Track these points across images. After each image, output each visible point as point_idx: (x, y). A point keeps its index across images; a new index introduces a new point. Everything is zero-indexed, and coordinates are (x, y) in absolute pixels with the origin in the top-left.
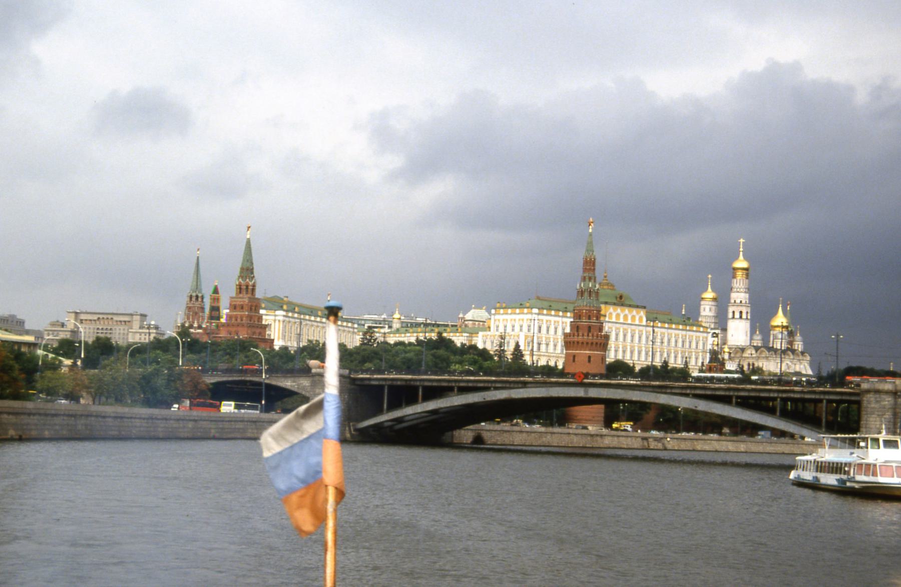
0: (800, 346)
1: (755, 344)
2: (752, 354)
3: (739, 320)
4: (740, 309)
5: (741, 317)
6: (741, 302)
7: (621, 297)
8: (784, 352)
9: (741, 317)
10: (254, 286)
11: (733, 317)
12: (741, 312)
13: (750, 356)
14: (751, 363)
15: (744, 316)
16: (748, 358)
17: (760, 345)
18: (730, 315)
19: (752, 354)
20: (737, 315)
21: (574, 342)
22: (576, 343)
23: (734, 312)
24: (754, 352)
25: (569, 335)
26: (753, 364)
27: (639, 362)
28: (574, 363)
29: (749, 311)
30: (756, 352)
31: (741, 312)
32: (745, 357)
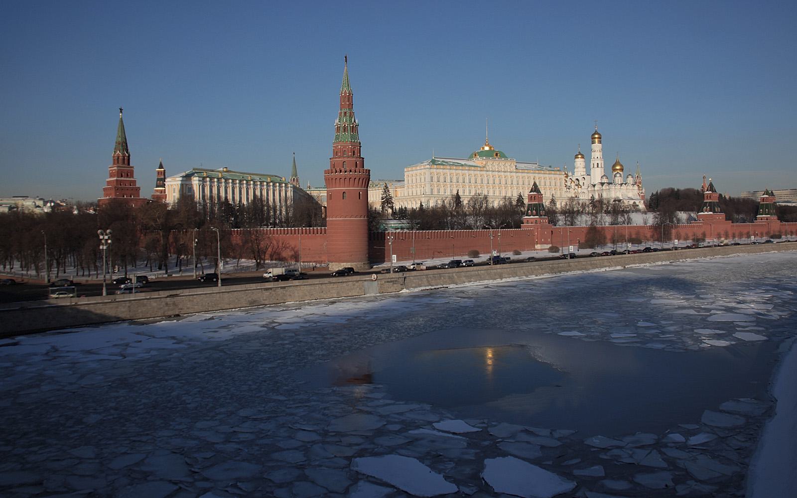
0: (631, 181)
1: (603, 182)
5: (598, 167)
9: (598, 167)
10: (129, 156)
12: (598, 164)
15: (600, 165)
17: (605, 182)
18: (592, 166)
20: (596, 166)
22: (330, 179)
24: (601, 186)
25: (330, 171)
27: (432, 196)
28: (331, 201)
29: (603, 163)
31: (598, 164)
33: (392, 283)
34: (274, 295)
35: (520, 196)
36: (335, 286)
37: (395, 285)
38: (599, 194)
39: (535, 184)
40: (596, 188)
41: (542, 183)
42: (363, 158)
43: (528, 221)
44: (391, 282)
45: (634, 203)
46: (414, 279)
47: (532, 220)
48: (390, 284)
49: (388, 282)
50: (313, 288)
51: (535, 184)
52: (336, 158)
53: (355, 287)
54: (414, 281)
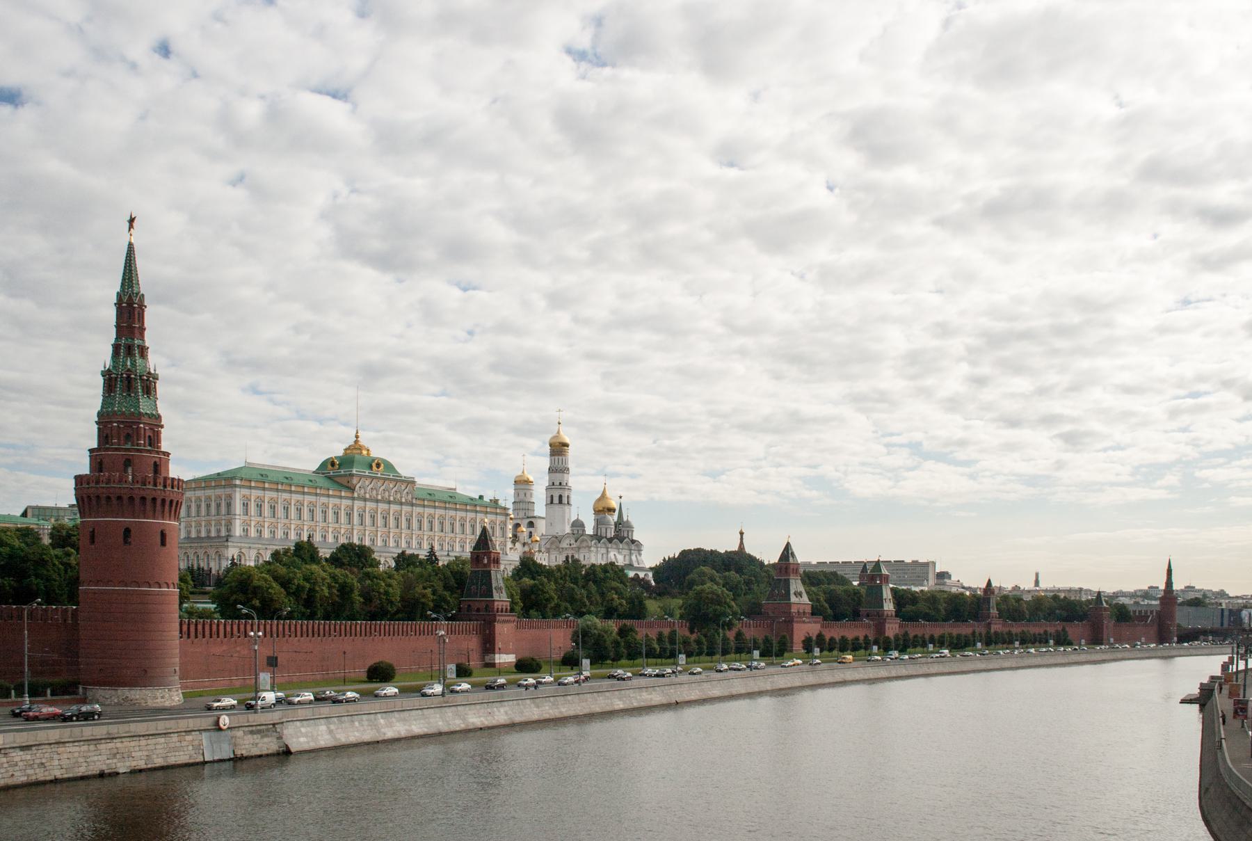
2: (570, 545)
3: (560, 506)
4: (560, 492)
5: (560, 502)
6: (560, 484)
7: (378, 465)
8: (610, 540)
9: (560, 502)
11: (552, 503)
12: (560, 497)
13: (569, 546)
14: (570, 556)
16: (566, 548)
19: (570, 545)
20: (556, 500)
21: (120, 498)
23: (552, 496)
24: (573, 542)
26: (573, 556)
30: (576, 541)
31: (560, 497)
32: (562, 548)
33: (259, 736)
34: (6, 765)
35: (432, 552)
36: (143, 742)
37: (266, 740)
38: (567, 557)
39: (484, 530)
40: (564, 544)
41: (498, 532)
42: (168, 454)
43: (469, 606)
44: (259, 732)
45: (636, 574)
46: (303, 726)
47: (477, 605)
48: (255, 736)
49: (252, 732)
50: (92, 747)
51: (484, 530)
52: (107, 449)
53: (184, 744)
54: (303, 730)
